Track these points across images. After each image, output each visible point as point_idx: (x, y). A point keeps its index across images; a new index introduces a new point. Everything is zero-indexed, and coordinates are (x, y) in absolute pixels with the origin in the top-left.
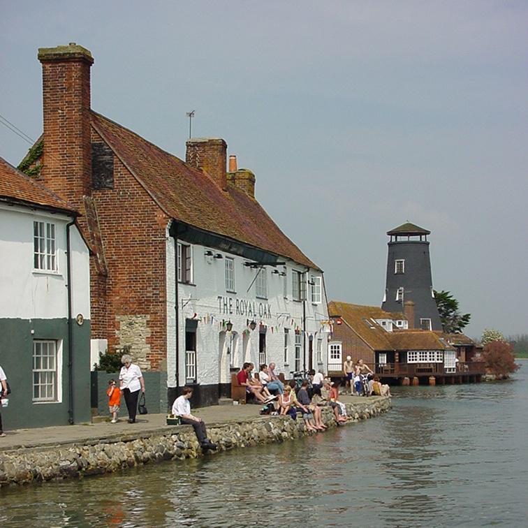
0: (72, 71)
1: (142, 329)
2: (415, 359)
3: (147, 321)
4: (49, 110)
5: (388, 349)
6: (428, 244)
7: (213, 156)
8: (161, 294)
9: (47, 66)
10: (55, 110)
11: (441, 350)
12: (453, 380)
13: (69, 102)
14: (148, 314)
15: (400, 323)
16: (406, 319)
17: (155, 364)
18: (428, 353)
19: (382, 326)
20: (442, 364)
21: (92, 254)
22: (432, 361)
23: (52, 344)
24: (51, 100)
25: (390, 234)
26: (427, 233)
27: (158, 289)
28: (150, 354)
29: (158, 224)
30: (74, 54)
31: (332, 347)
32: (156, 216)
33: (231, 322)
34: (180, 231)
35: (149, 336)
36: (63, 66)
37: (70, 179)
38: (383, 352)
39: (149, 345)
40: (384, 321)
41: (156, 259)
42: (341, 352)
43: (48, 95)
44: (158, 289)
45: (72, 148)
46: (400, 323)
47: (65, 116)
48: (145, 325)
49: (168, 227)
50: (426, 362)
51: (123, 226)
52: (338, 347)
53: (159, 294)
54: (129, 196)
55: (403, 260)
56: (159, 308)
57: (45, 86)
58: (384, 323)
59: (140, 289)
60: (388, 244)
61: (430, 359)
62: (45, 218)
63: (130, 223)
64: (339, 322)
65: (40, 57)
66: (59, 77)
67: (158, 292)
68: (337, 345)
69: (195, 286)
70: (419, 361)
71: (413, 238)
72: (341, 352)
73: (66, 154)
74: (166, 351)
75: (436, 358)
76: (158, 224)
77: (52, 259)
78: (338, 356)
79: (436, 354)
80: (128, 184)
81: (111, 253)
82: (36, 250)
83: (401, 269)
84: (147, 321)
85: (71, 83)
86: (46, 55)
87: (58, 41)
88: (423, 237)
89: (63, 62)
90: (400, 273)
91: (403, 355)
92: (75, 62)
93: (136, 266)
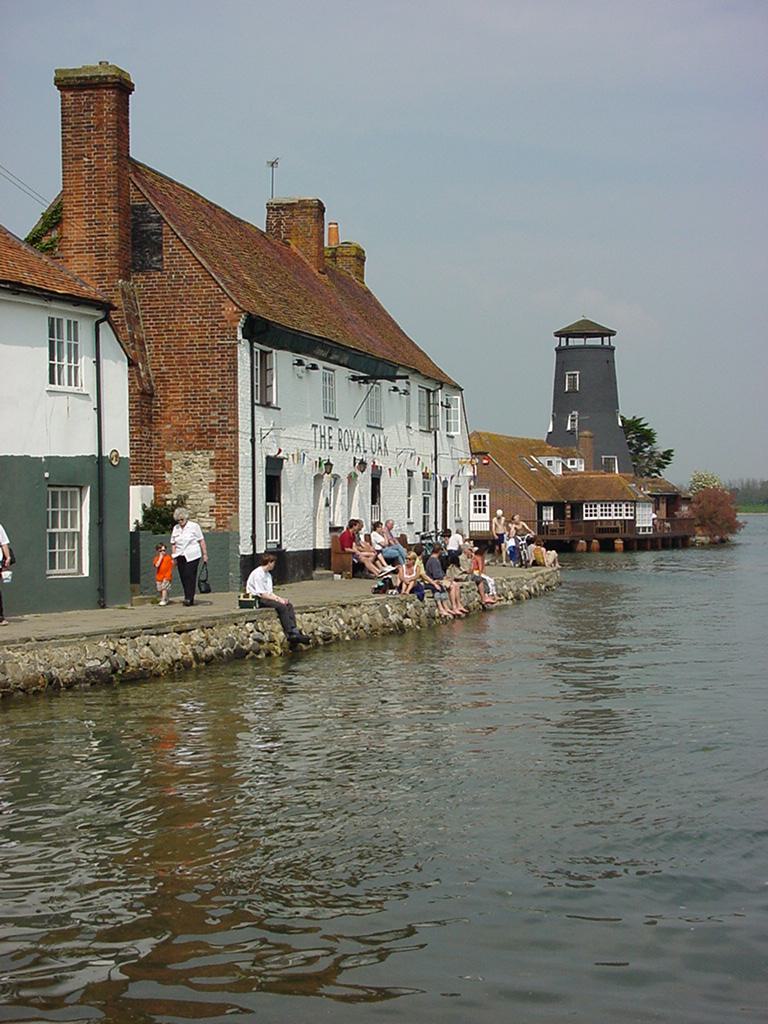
0: (104, 102)
1: (204, 470)
2: (594, 514)
3: (211, 460)
4: (70, 158)
5: (555, 500)
6: (613, 349)
7: (305, 224)
8: (231, 421)
9: (68, 95)
10: (78, 158)
11: (632, 501)
12: (649, 544)
13: (100, 147)
14: (211, 449)
15: (572, 463)
16: (581, 457)
17: (222, 521)
18: (613, 505)
19: (547, 466)
20: (634, 521)
21: (132, 364)
22: (618, 518)
23: (75, 492)
24: (73, 144)
25: (559, 334)
26: (611, 333)
27: (227, 414)
28: (214, 507)
29: (226, 321)
30: (106, 77)
31: (475, 496)
32: (224, 309)
33: (331, 461)
34: (258, 330)
35: (214, 481)
36: (91, 95)
37: (100, 256)
38: (548, 504)
39: (214, 495)
40: (550, 459)
41: (223, 371)
42: (488, 503)
43: (69, 136)
44: (227, 414)
45: (104, 212)
46: (572, 463)
47: (93, 166)
48: (208, 465)
49: (240, 324)
50: (610, 518)
51: (176, 323)
52: (484, 497)
53: (227, 421)
54: (185, 280)
55: (578, 372)
56: (228, 441)
57: (64, 124)
58: (550, 463)
59: (201, 414)
60: (556, 349)
61: (616, 514)
62: (64, 312)
63: (186, 319)
64: (485, 461)
65: (57, 81)
66: (85, 111)
67: (226, 419)
68: (482, 494)
69: (279, 409)
70: (599, 518)
71: (591, 341)
72: (488, 503)
73: (94, 220)
74: (238, 503)
75: (624, 512)
76: (226, 321)
77: (74, 372)
78: (484, 510)
79: (624, 507)
80: (183, 264)
81: (159, 362)
82: (52, 358)
83: (575, 386)
84: (211, 460)
85: (101, 120)
86: (65, 78)
87: (83, 59)
88: (606, 339)
89: (91, 89)
90: (573, 391)
91: (577, 508)
92: (107, 89)
93: (195, 381)
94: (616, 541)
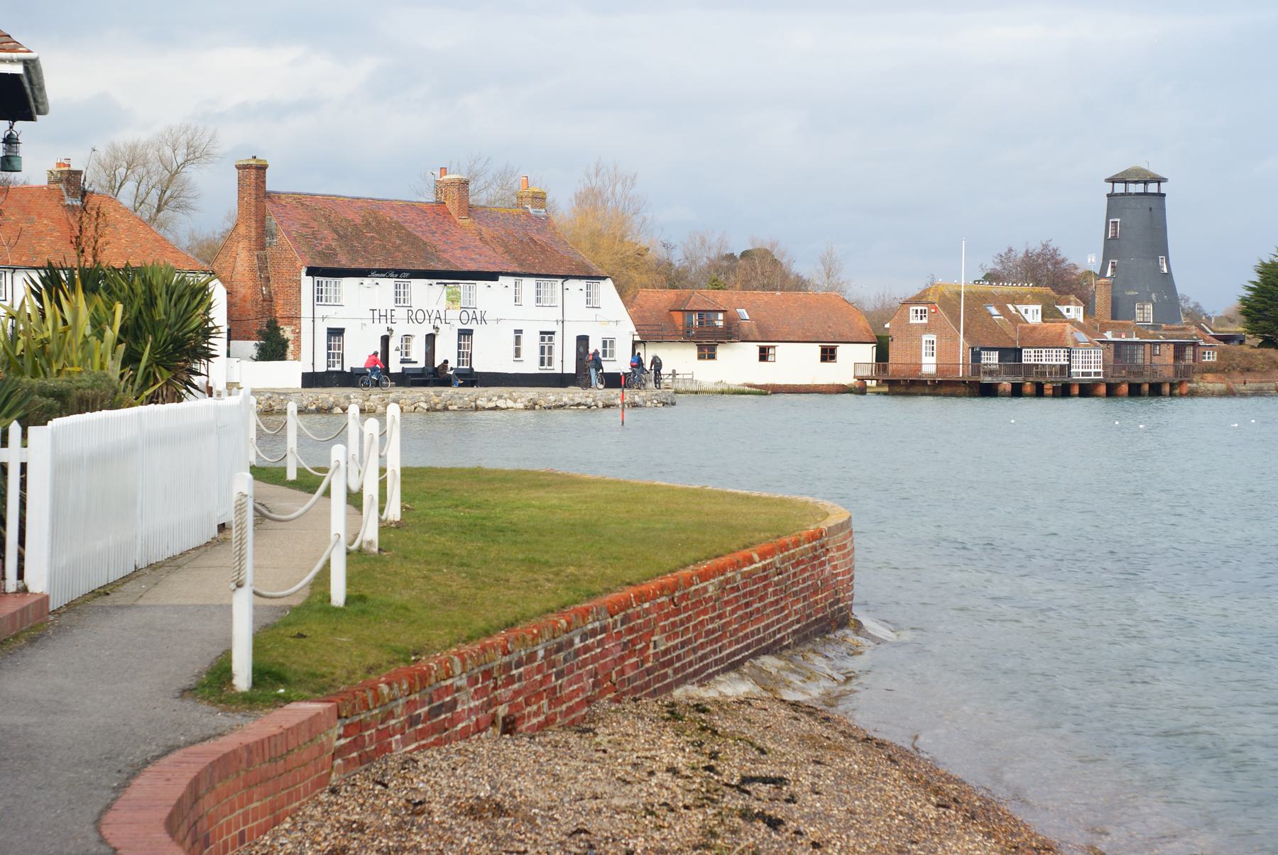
4: (241, 198)
6: (1164, 195)
7: (453, 192)
10: (243, 199)
11: (1068, 348)
21: (228, 293)
25: (1113, 181)
26: (1159, 181)
34: (312, 272)
46: (1068, 310)
55: (1118, 220)
57: (239, 184)
58: (1026, 311)
60: (1108, 195)
61: (1055, 358)
64: (933, 310)
70: (1044, 362)
75: (1062, 358)
83: (1116, 233)
87: (245, 159)
90: (1114, 238)
94: (1046, 387)
